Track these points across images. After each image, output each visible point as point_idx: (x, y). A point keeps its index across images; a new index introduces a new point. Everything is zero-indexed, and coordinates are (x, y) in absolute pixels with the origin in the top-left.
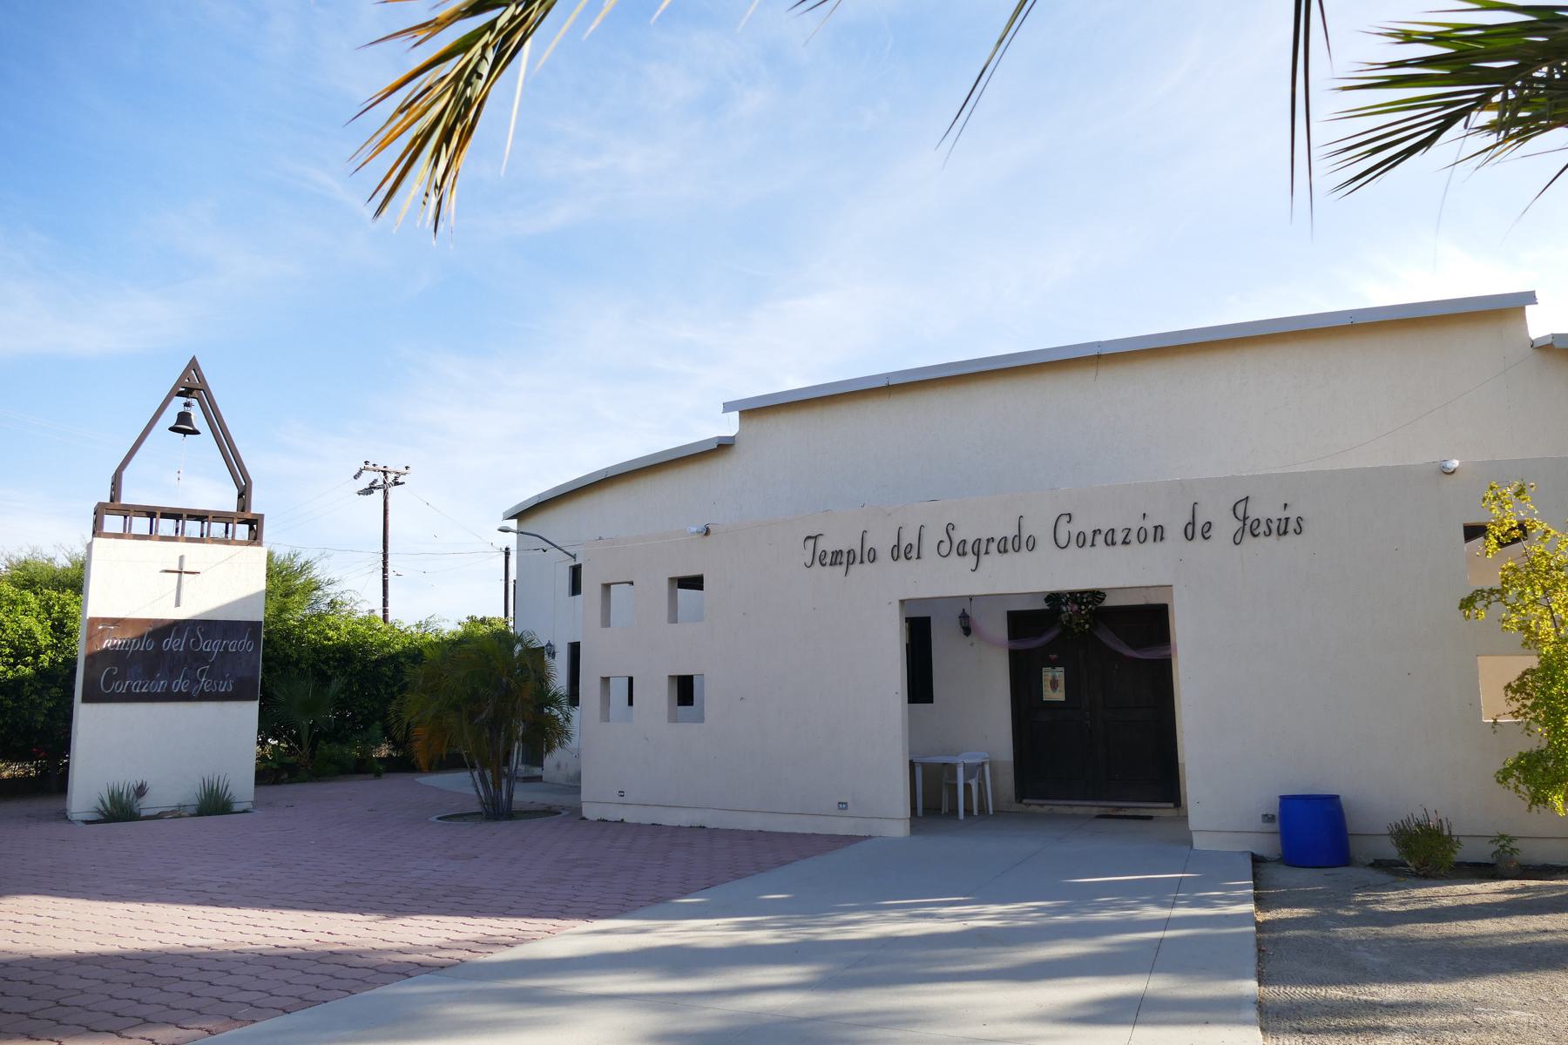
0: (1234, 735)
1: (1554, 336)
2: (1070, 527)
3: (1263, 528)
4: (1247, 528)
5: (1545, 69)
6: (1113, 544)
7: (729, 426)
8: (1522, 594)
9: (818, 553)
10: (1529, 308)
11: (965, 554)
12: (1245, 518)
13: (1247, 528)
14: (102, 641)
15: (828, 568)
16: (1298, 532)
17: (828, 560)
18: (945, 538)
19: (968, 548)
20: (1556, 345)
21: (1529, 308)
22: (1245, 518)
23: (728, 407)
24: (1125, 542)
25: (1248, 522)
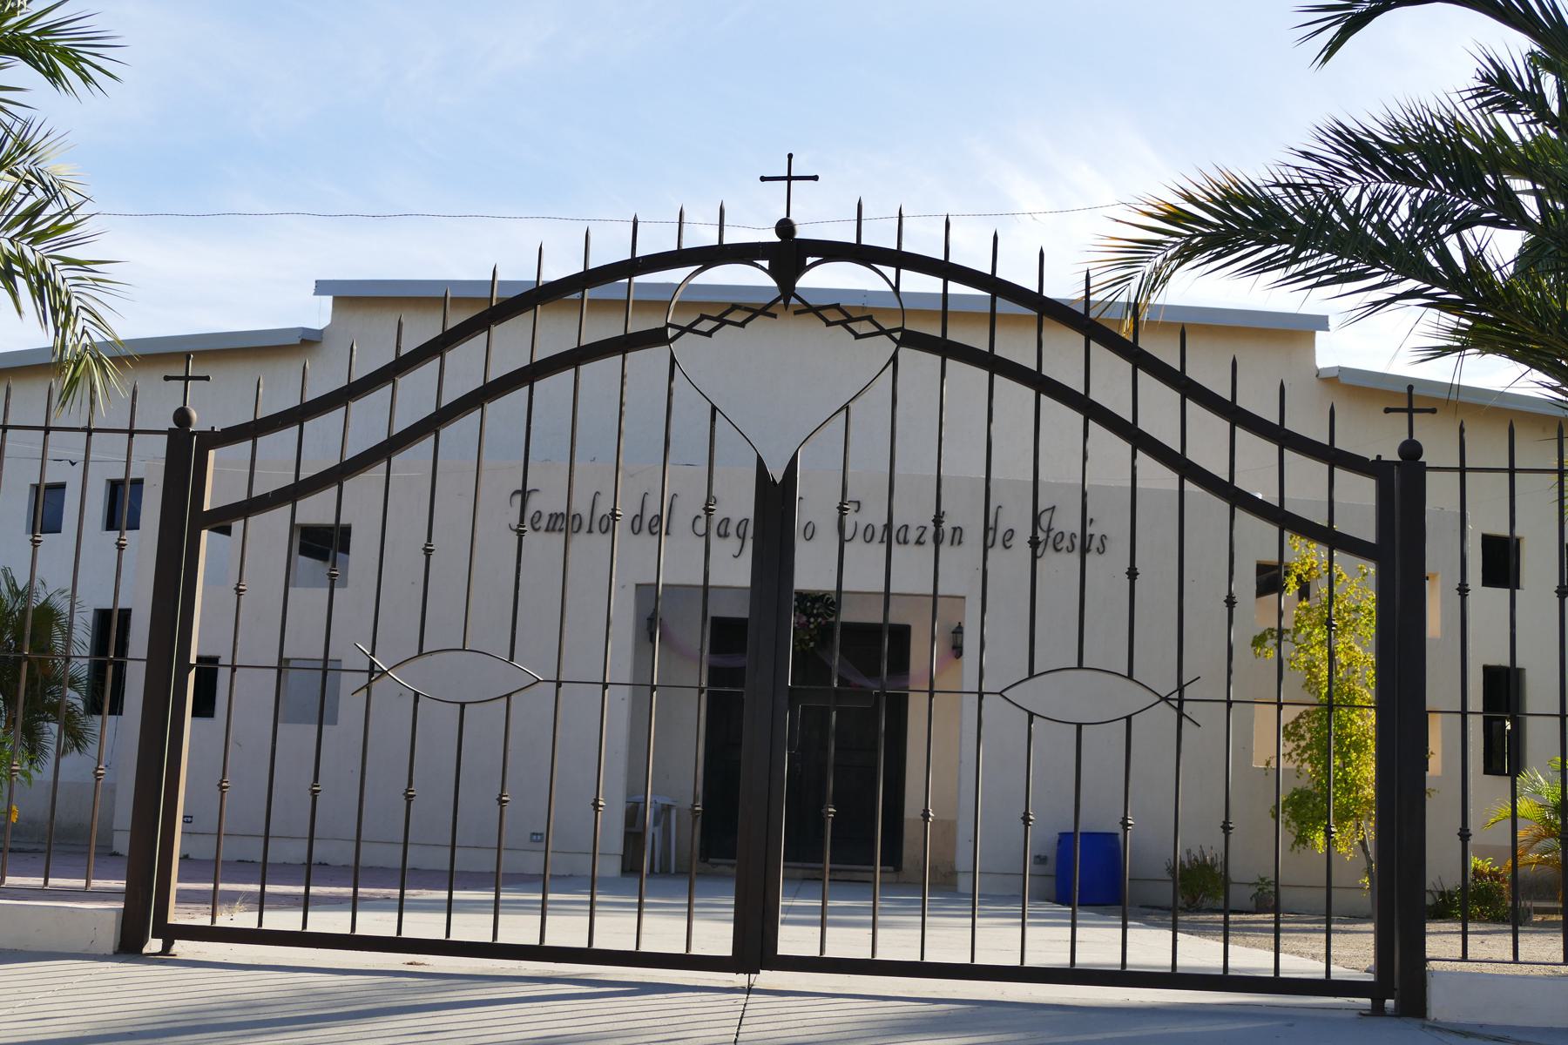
0: (963, 759)
1: (1341, 369)
2: (857, 517)
3: (1066, 543)
4: (1050, 541)
5: (1518, 184)
6: (906, 542)
7: (318, 314)
8: (1309, 635)
9: (529, 514)
10: (1319, 334)
11: (726, 535)
12: (1049, 530)
13: (1050, 541)
14: (1350, 787)
15: (542, 534)
16: (1101, 551)
17: (543, 523)
18: (702, 513)
19: (732, 529)
20: (1342, 380)
21: (1319, 334)
22: (1049, 530)
23: (322, 287)
24: (919, 542)
25: (1052, 534)
